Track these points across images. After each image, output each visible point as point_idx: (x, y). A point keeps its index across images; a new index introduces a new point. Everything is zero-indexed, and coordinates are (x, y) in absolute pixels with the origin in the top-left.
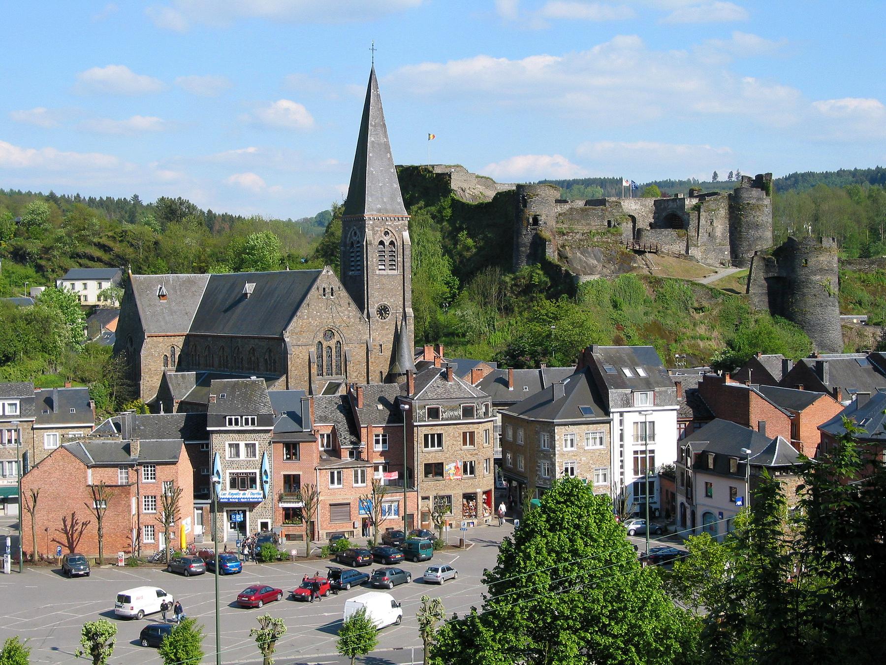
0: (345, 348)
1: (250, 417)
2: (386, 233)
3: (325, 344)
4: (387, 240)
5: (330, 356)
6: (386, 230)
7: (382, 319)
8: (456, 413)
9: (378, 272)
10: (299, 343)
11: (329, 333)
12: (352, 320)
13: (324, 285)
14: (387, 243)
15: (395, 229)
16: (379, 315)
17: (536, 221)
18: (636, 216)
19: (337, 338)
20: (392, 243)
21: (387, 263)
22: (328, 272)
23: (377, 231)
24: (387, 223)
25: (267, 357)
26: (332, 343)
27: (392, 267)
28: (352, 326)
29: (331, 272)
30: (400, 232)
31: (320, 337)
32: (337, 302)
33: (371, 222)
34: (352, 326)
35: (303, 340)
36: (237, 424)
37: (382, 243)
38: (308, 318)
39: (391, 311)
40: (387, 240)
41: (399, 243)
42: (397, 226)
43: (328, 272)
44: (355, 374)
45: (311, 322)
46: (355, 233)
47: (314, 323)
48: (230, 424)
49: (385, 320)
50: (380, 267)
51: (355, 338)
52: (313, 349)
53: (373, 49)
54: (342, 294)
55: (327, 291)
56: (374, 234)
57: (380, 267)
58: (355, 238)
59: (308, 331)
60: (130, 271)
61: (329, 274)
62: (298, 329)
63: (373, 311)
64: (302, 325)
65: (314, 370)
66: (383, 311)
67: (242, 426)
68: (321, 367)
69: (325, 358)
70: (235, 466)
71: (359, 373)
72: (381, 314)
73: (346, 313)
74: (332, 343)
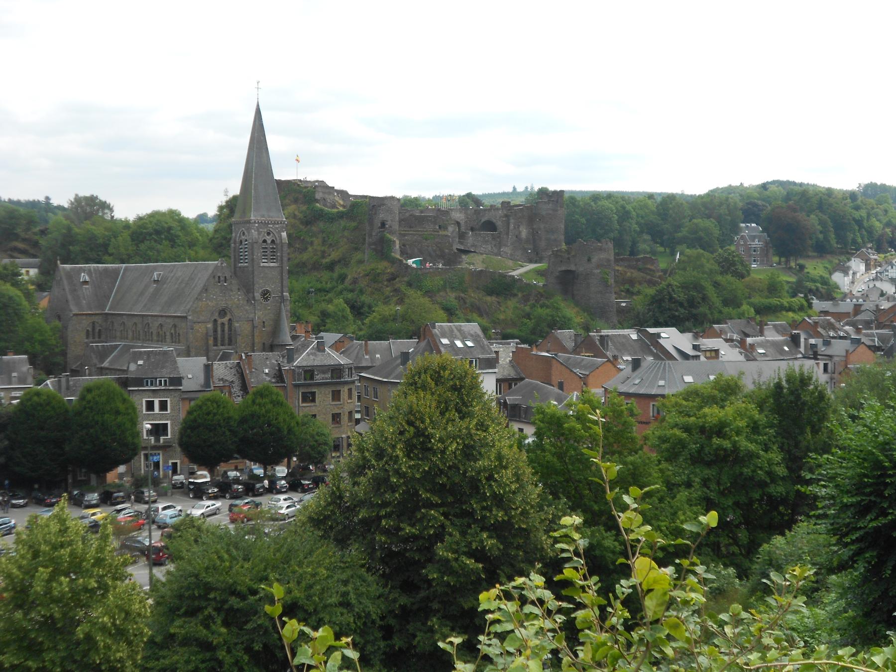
1: (163, 380)
2: (268, 234)
3: (220, 321)
4: (269, 239)
5: (223, 331)
8: (326, 376)
10: (199, 320)
11: (223, 313)
12: (241, 302)
13: (219, 274)
14: (269, 242)
17: (383, 225)
18: (461, 222)
20: (273, 241)
25: (173, 331)
26: (225, 320)
30: (279, 233)
31: (216, 316)
32: (229, 287)
35: (202, 318)
36: (152, 385)
37: (265, 241)
40: (269, 239)
41: (278, 241)
42: (277, 228)
44: (243, 345)
46: (244, 234)
48: (147, 385)
52: (210, 326)
54: (233, 282)
55: (222, 279)
56: (259, 233)
58: (243, 237)
60: (59, 262)
63: (258, 295)
65: (211, 342)
66: (265, 294)
67: (156, 386)
68: (215, 339)
69: (219, 332)
70: (151, 418)
74: (225, 320)
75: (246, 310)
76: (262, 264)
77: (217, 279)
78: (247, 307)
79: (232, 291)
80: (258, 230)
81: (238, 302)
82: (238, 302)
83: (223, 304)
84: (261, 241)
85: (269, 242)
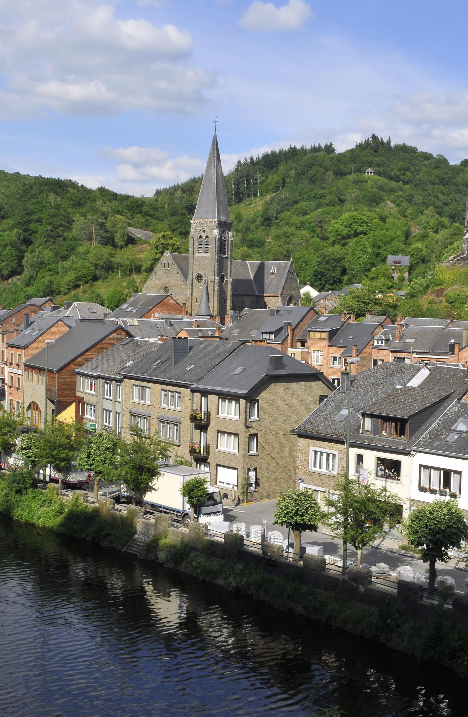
2: (204, 231)
9: (197, 254)
14: (204, 237)
15: (208, 228)
20: (207, 237)
21: (203, 249)
22: (167, 254)
27: (206, 251)
28: (178, 286)
29: (169, 254)
30: (211, 230)
32: (171, 271)
33: (195, 225)
34: (178, 286)
37: (201, 237)
38: (155, 280)
39: (204, 278)
42: (210, 227)
43: (167, 254)
50: (200, 251)
51: (180, 293)
53: (216, 122)
55: (166, 265)
57: (200, 251)
61: (168, 255)
62: (149, 286)
66: (199, 278)
72: (198, 280)
73: (176, 278)
75: (182, 289)
76: (197, 254)
77: (163, 265)
79: (173, 274)
80: (195, 229)
81: (176, 282)
83: (166, 283)
84: (197, 237)
85: (204, 237)
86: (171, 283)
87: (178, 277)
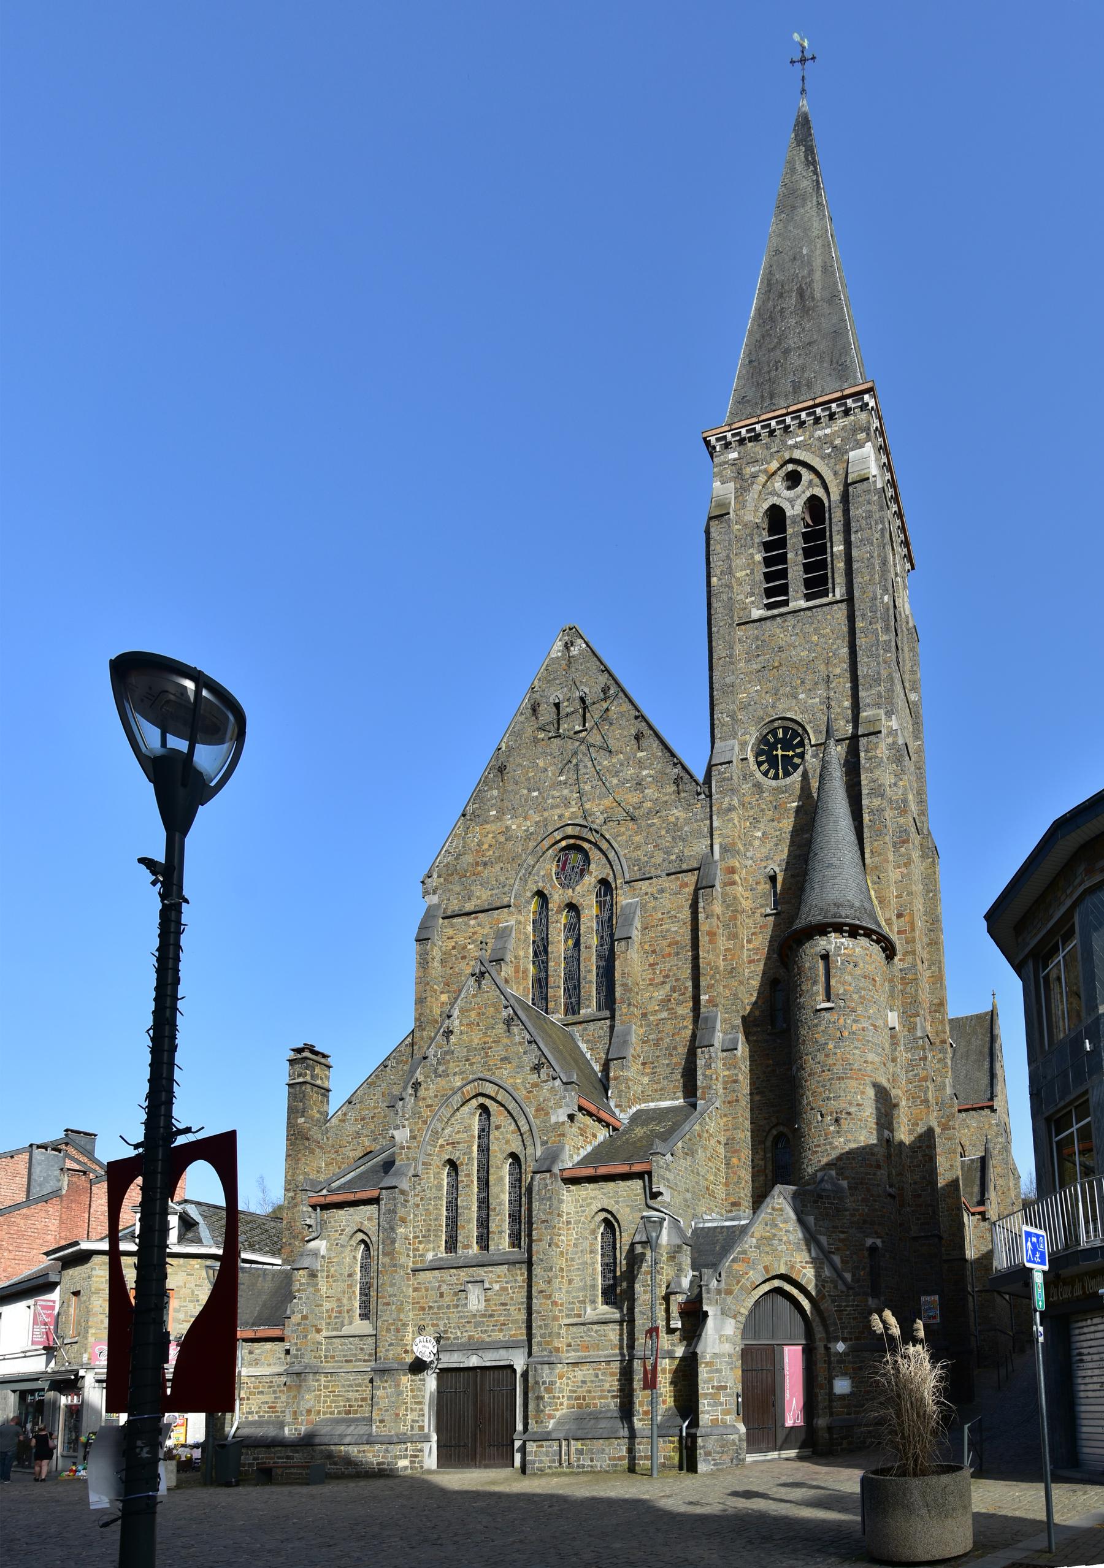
0: (624, 899)
3: (558, 897)
6: (790, 467)
7: (765, 774)
13: (557, 694)
16: (765, 767)
19: (598, 869)
23: (755, 476)
24: (790, 442)
33: (734, 455)
42: (827, 440)
45: (508, 828)
47: (519, 826)
49: (788, 780)
59: (499, 859)
62: (469, 858)
64: (480, 844)
71: (673, 989)
72: (773, 761)
75: (674, 828)
78: (677, 813)
81: (633, 798)
82: (633, 798)
86: (597, 809)
87: (641, 765)
